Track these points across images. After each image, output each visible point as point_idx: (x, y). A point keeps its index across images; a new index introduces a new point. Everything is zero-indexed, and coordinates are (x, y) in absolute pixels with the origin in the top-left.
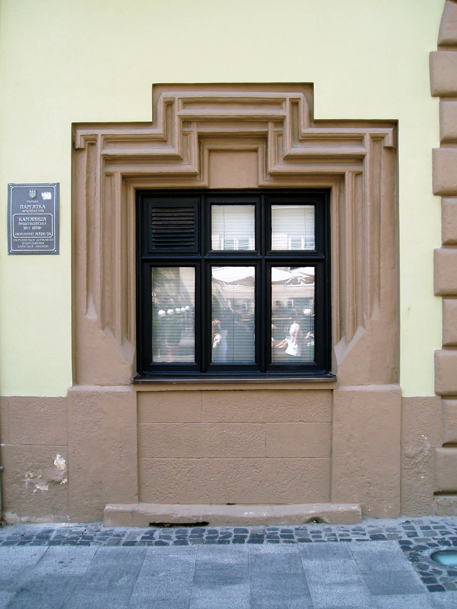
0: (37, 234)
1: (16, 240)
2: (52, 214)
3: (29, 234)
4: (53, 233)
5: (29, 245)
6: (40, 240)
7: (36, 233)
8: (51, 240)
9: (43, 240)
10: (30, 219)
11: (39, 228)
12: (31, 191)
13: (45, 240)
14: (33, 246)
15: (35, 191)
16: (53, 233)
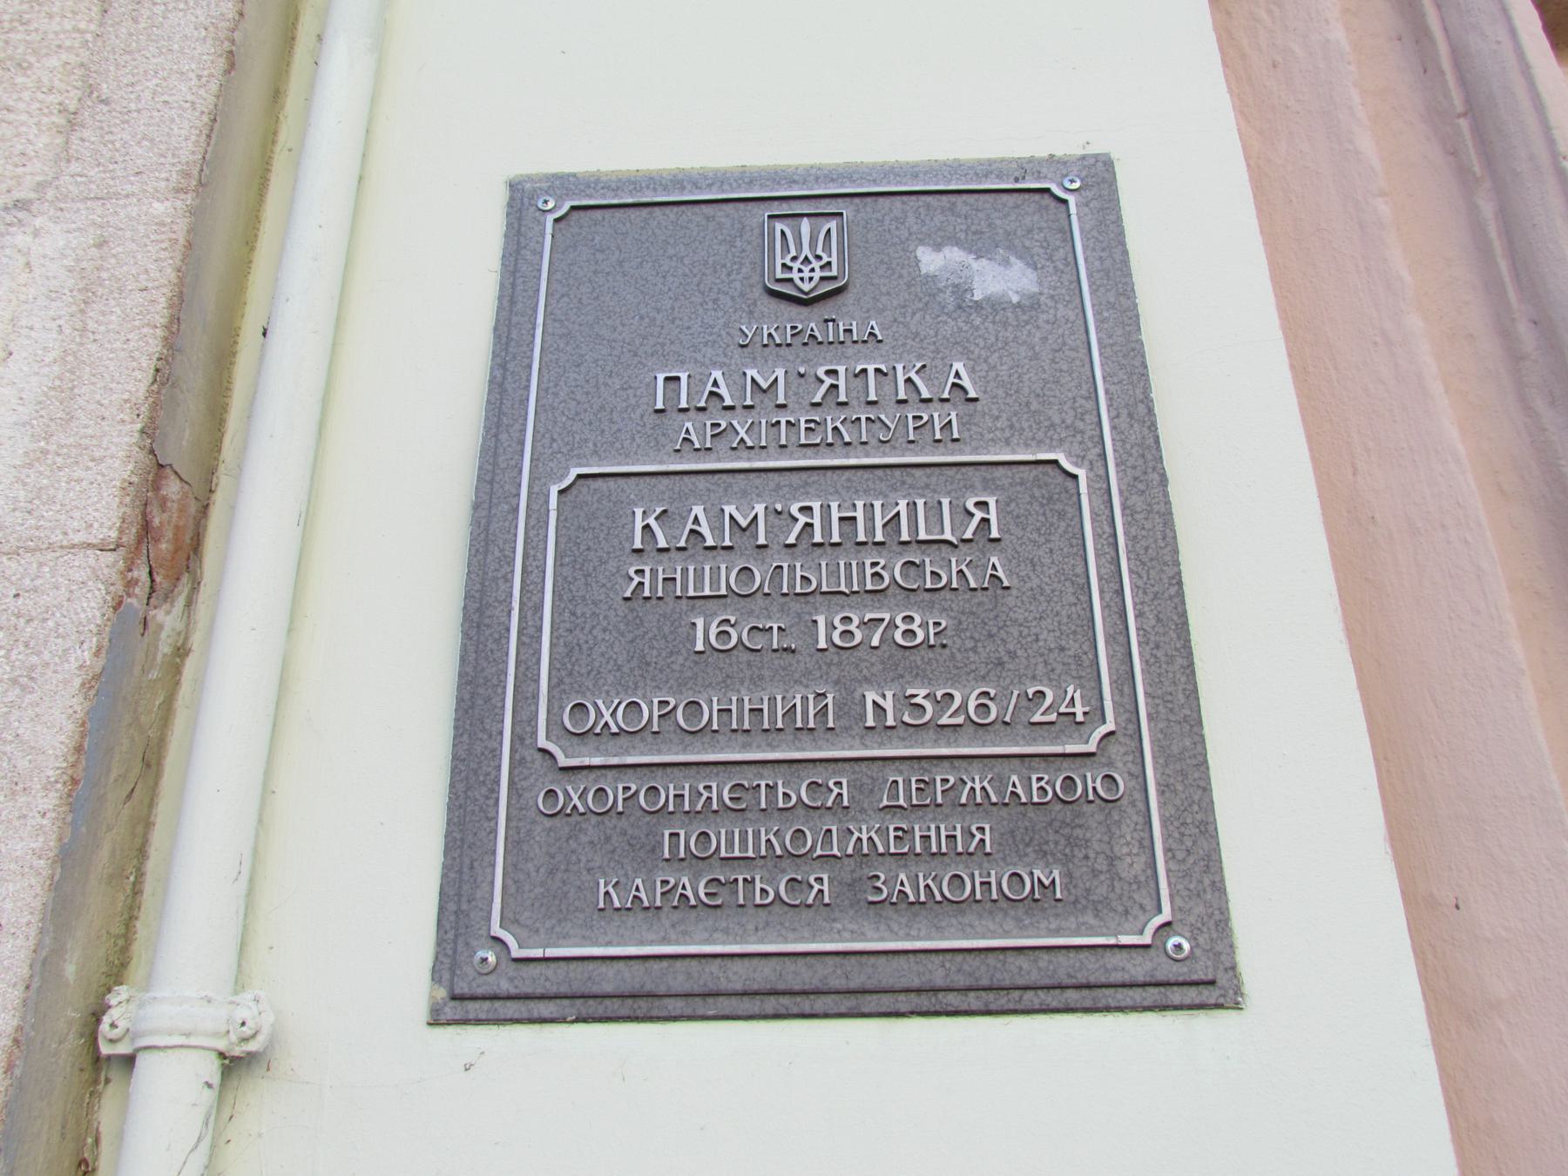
0: (888, 705)
1: (573, 794)
2: (1079, 460)
3: (776, 700)
4: (1124, 680)
5: (774, 860)
6: (925, 786)
7: (871, 696)
8: (1093, 780)
9: (978, 781)
10: (780, 516)
11: (923, 625)
12: (779, 226)
13: (1000, 782)
14: (823, 883)
15: (833, 224)
16: (1124, 680)
